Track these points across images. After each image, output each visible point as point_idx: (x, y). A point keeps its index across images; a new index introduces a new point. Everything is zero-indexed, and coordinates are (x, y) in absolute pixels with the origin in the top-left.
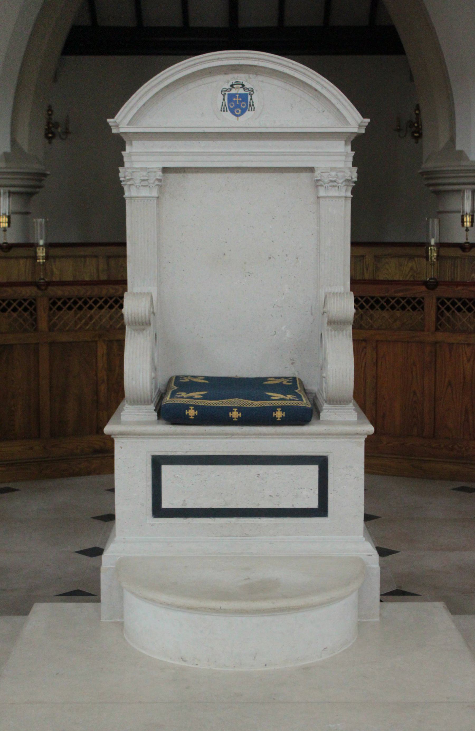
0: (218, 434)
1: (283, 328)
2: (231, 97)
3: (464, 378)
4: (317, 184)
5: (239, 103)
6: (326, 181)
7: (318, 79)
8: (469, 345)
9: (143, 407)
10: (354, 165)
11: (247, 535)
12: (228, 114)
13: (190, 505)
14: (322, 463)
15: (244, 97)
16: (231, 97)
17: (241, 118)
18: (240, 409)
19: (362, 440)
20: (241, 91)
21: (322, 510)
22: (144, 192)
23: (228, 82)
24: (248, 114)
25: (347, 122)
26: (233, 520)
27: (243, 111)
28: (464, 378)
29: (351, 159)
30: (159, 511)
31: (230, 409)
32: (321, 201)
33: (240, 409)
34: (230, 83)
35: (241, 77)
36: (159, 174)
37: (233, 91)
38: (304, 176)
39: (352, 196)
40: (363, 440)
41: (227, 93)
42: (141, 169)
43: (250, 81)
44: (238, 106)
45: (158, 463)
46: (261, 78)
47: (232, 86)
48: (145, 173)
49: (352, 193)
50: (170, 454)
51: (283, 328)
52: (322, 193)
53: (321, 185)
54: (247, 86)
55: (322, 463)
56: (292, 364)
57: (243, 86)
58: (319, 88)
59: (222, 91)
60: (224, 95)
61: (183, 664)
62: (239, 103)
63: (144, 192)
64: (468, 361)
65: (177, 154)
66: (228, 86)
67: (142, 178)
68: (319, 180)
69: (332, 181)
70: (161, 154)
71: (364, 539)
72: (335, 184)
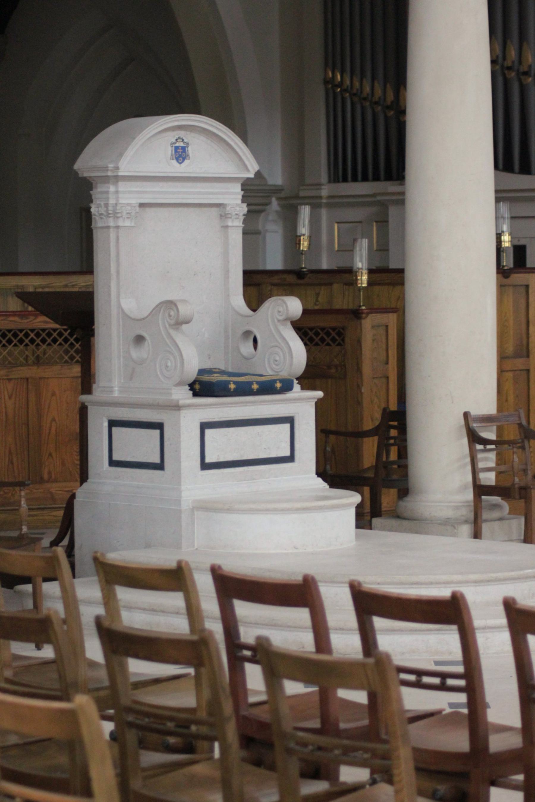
0: (231, 403)
1: (203, 330)
2: (177, 148)
3: (7, 416)
4: (224, 216)
5: (181, 154)
6: (234, 214)
7: (233, 137)
8: (10, 380)
9: (183, 387)
10: (243, 202)
11: (254, 479)
12: (174, 162)
13: (222, 459)
14: (290, 420)
15: (184, 148)
16: (177, 148)
17: (182, 164)
18: (257, 383)
19: (313, 404)
20: (182, 144)
21: (291, 459)
22: (127, 223)
23: (174, 137)
24: (186, 162)
25: (248, 170)
26: (245, 468)
27: (184, 159)
28: (7, 416)
29: (240, 197)
30: (205, 466)
31: (251, 383)
32: (230, 230)
33: (257, 383)
34: (175, 138)
35: (182, 133)
36: (138, 209)
37: (177, 144)
38: (214, 210)
39: (243, 225)
40: (314, 403)
41: (174, 145)
42: (128, 204)
43: (188, 137)
44: (180, 156)
45: (204, 426)
46: (193, 134)
47: (177, 140)
48: (129, 208)
49: (243, 223)
50: (211, 420)
51: (203, 330)
52: (230, 224)
53: (231, 218)
54: (185, 141)
55: (290, 420)
56: (209, 358)
57: (183, 140)
58: (232, 143)
59: (171, 144)
60: (172, 147)
61: (295, 551)
62: (181, 154)
63: (127, 223)
64: (10, 398)
65: (146, 192)
66: (174, 141)
67: (128, 212)
68: (230, 214)
69: (237, 214)
70: (138, 192)
71: (316, 476)
72: (237, 216)
